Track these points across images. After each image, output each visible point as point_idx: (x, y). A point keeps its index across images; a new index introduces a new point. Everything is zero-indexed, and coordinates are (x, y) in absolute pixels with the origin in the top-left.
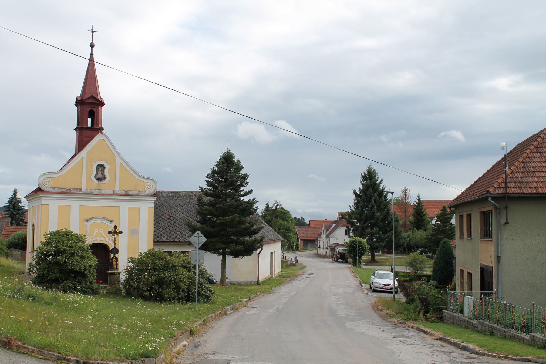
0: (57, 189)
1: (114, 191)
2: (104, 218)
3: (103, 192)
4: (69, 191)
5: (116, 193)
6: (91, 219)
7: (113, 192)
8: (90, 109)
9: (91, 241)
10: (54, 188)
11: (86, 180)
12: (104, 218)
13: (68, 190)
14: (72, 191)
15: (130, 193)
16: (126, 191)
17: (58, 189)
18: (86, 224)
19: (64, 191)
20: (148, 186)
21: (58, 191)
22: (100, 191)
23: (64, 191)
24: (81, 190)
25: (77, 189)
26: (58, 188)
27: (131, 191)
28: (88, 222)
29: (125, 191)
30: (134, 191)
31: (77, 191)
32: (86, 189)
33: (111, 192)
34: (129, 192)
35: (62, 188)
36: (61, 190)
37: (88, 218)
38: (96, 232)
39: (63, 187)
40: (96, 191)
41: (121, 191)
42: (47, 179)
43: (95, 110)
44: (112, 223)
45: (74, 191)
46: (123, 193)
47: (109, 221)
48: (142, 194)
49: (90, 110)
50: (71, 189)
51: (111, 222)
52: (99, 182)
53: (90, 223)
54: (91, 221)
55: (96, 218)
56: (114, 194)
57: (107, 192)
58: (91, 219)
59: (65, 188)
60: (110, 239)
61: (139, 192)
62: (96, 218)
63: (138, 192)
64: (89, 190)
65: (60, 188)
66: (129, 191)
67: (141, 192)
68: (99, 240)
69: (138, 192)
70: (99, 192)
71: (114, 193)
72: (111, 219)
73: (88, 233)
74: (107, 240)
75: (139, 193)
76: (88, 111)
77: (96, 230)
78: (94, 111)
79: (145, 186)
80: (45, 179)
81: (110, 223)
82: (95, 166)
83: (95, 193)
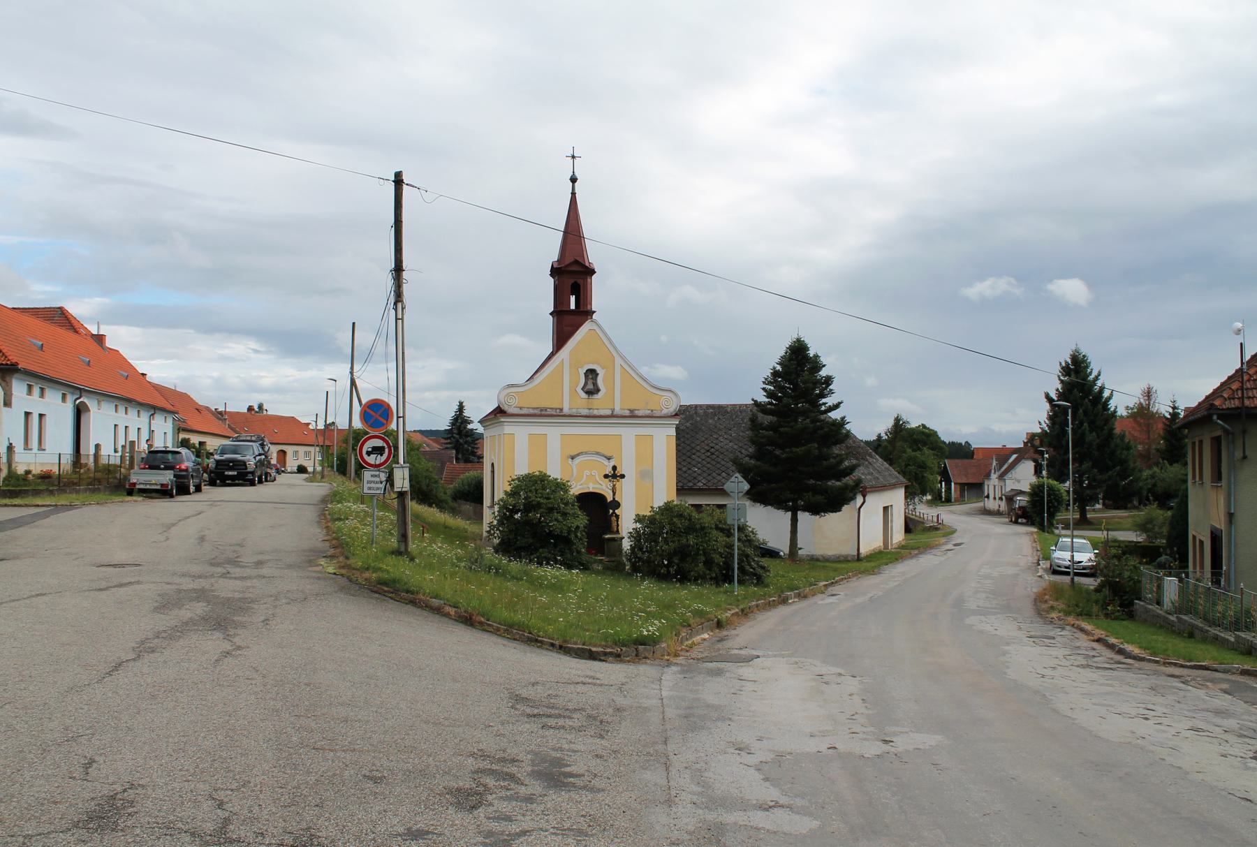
2: (597, 453)
3: (596, 412)
4: (543, 413)
5: (615, 413)
6: (578, 455)
9: (580, 489)
10: (521, 408)
12: (597, 453)
13: (542, 410)
14: (549, 412)
16: (631, 411)
18: (570, 463)
22: (591, 411)
23: (537, 412)
24: (561, 410)
25: (556, 409)
26: (528, 408)
31: (556, 412)
33: (609, 412)
34: (636, 412)
35: (534, 409)
36: (532, 411)
40: (585, 412)
46: (627, 413)
47: (605, 457)
51: (609, 459)
53: (577, 460)
55: (586, 453)
56: (612, 416)
57: (602, 412)
58: (578, 455)
59: (538, 408)
61: (652, 411)
62: (586, 453)
63: (650, 411)
66: (636, 410)
68: (591, 488)
69: (650, 411)
71: (612, 413)
72: (609, 455)
73: (574, 476)
74: (604, 487)
80: (508, 395)
82: (582, 372)
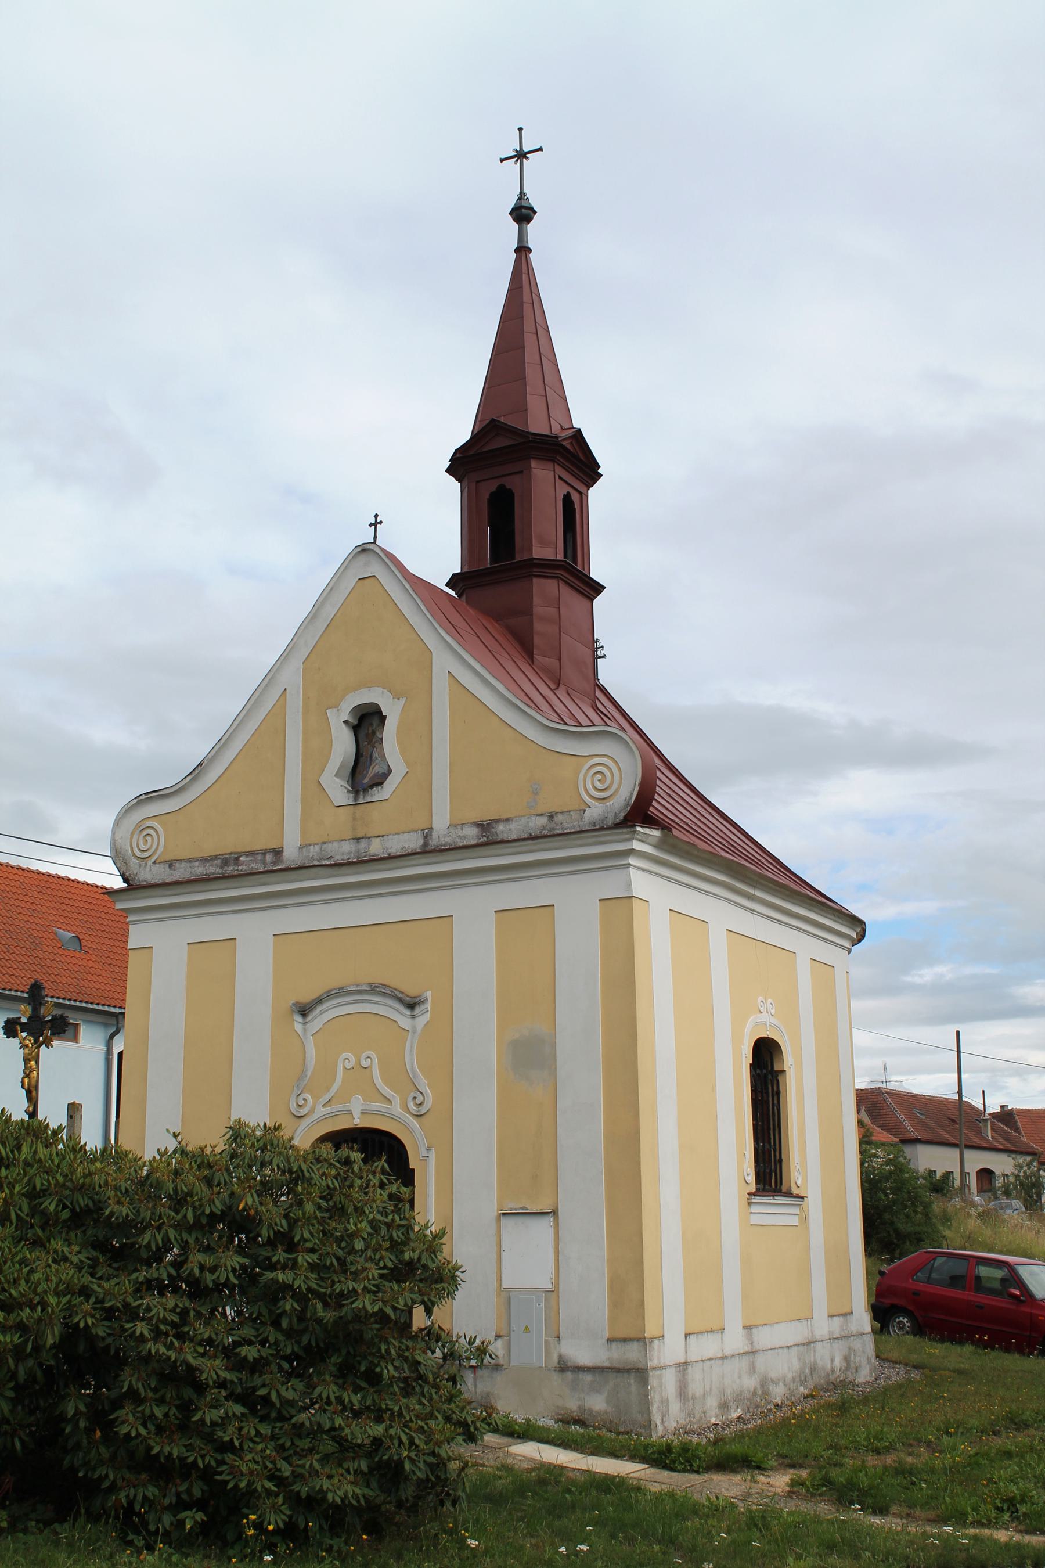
0: (183, 864)
1: (425, 837)
2: (375, 989)
3: (376, 848)
4: (230, 869)
5: (434, 842)
6: (319, 1001)
7: (421, 842)
8: (492, 486)
9: (323, 1119)
10: (171, 864)
11: (304, 801)
12: (375, 989)
13: (225, 862)
14: (247, 864)
15: (502, 830)
16: (484, 827)
17: (188, 865)
18: (298, 1027)
19: (212, 870)
20: (599, 777)
21: (187, 876)
22: (363, 844)
23: (213, 869)
24: (278, 853)
25: (264, 852)
26: (189, 860)
27: (508, 820)
28: (309, 1019)
29: (479, 825)
30: (523, 821)
31: (264, 862)
32: (301, 848)
33: (414, 842)
34: (501, 827)
35: (205, 860)
36: (199, 870)
37: (306, 997)
38: (344, 1067)
39: (209, 851)
40: (344, 850)
41: (459, 832)
42: (149, 823)
43: (510, 482)
44: (417, 1011)
45: (254, 865)
46: (471, 834)
47: (400, 1000)
48: (567, 823)
49: (494, 489)
50: (237, 859)
51: (411, 1006)
52: (356, 799)
53: (319, 1019)
54: (321, 1013)
55: (341, 992)
56: (427, 851)
57: (396, 845)
58: (319, 1001)
59: (216, 857)
60: (412, 1106)
61: (551, 817)
62: (341, 992)
63: (544, 821)
64: (314, 850)
65: (196, 860)
66: (498, 821)
67: (560, 818)
68: (356, 1114)
69: (544, 821)
70: (358, 851)
71: (425, 845)
72: (411, 990)
73: (309, 1074)
74: (397, 1109)
75: (553, 825)
76: (487, 496)
77: (347, 1059)
78: (510, 490)
79: (581, 777)
80: (142, 828)
81: (408, 1012)
82: (343, 713)
83: (338, 858)
